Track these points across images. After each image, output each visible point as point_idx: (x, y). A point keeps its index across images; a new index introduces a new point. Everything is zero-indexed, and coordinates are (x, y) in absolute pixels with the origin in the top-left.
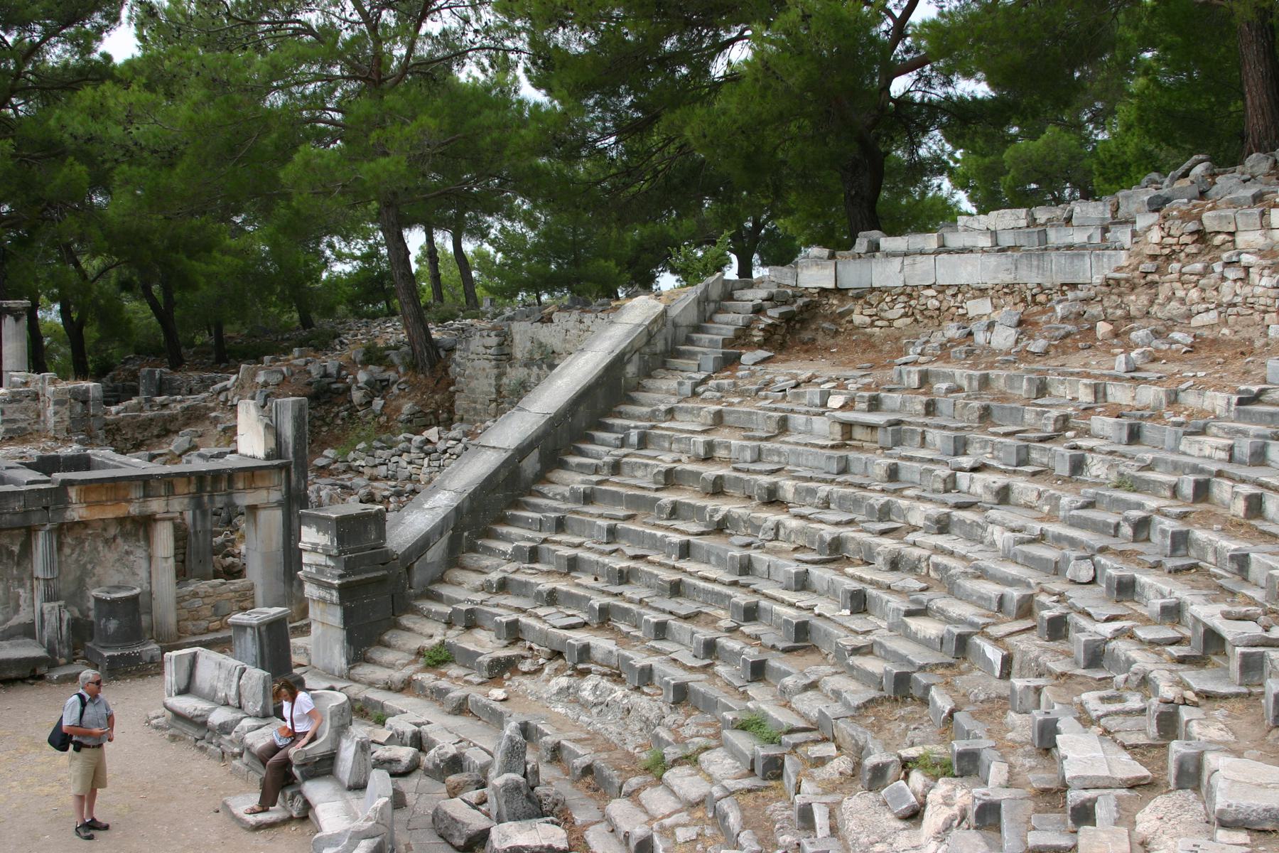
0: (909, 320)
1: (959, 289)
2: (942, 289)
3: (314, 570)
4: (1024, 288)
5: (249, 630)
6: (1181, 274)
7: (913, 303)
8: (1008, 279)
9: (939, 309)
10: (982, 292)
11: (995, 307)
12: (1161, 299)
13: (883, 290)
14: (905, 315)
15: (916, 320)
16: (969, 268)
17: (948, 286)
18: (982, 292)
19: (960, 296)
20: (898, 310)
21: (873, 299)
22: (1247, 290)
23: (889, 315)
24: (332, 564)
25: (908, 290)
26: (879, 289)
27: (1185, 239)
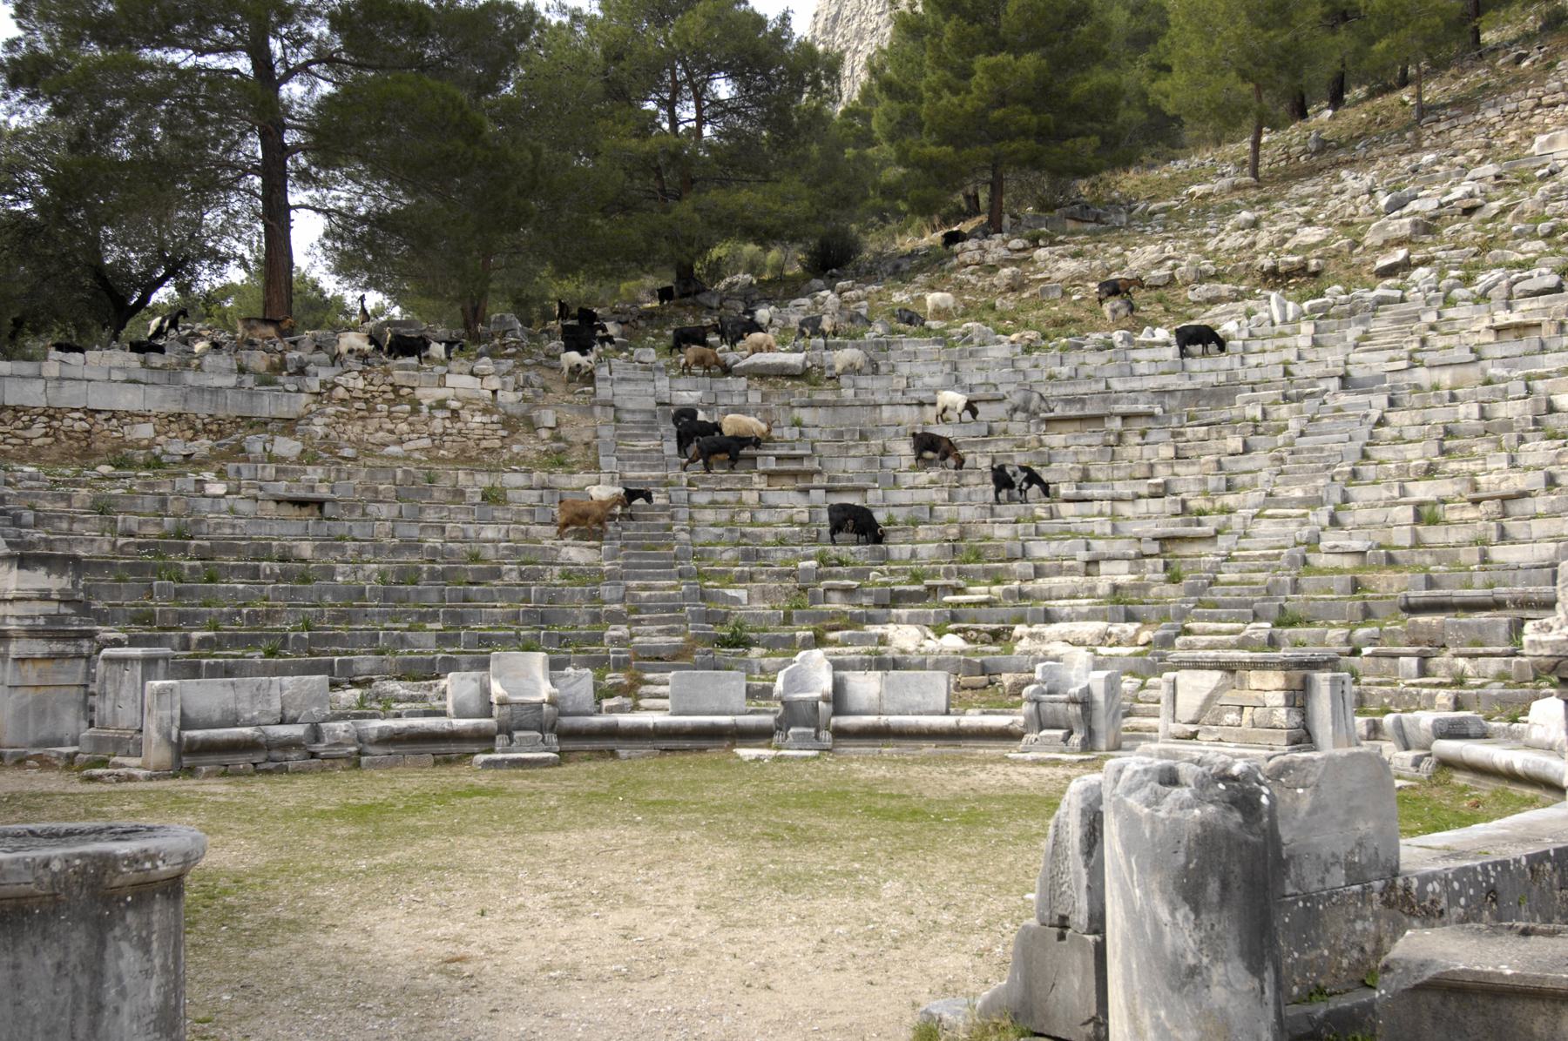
0: (49, 440)
1: (114, 414)
2: (92, 412)
3: (42, 621)
4: (192, 417)
5: (161, 662)
6: (390, 413)
7: (55, 424)
8: (176, 409)
9: (89, 432)
10: (145, 417)
11: (158, 433)
12: (371, 429)
13: (25, 410)
14: (46, 435)
15: (57, 440)
16: (130, 396)
17: (99, 412)
18: (145, 417)
19: (114, 421)
20: (38, 429)
21: (7, 416)
22: (459, 425)
23: (27, 434)
24: (70, 611)
25: (51, 412)
26: (15, 409)
27: (383, 388)
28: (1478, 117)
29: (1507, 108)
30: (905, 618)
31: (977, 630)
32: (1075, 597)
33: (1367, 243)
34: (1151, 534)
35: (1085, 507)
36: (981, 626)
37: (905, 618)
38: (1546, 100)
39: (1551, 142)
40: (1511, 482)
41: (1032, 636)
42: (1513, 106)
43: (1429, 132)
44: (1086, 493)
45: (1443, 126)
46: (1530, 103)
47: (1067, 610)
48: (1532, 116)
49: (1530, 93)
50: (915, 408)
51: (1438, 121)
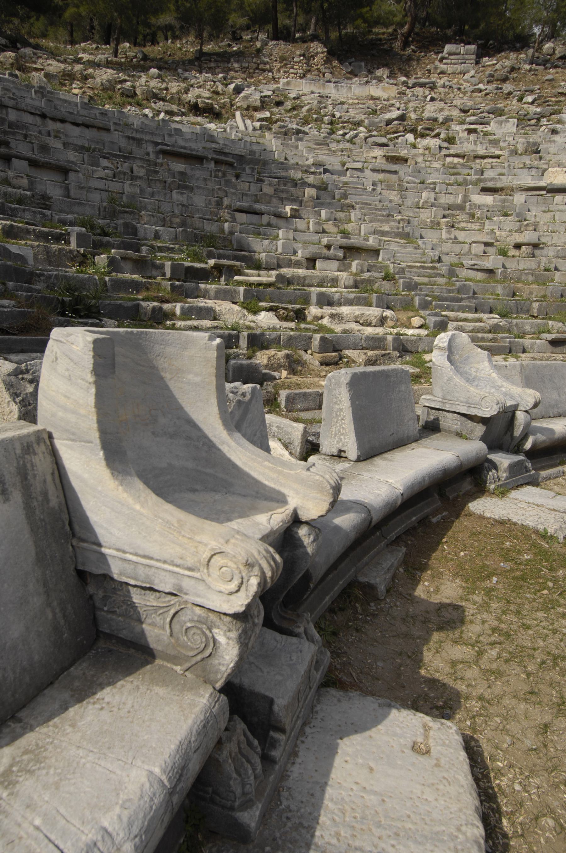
28: (230, 65)
29: (244, 65)
30: (212, 293)
31: (286, 309)
32: (322, 286)
33: (238, 105)
34: (339, 243)
35: (255, 218)
36: (290, 306)
37: (212, 293)
38: (261, 66)
39: (288, 83)
40: (513, 237)
41: (332, 316)
42: (247, 65)
43: (205, 66)
44: (257, 206)
45: (213, 65)
46: (255, 66)
47: (337, 296)
48: (254, 73)
49: (254, 60)
50: (38, 119)
51: (210, 61)
